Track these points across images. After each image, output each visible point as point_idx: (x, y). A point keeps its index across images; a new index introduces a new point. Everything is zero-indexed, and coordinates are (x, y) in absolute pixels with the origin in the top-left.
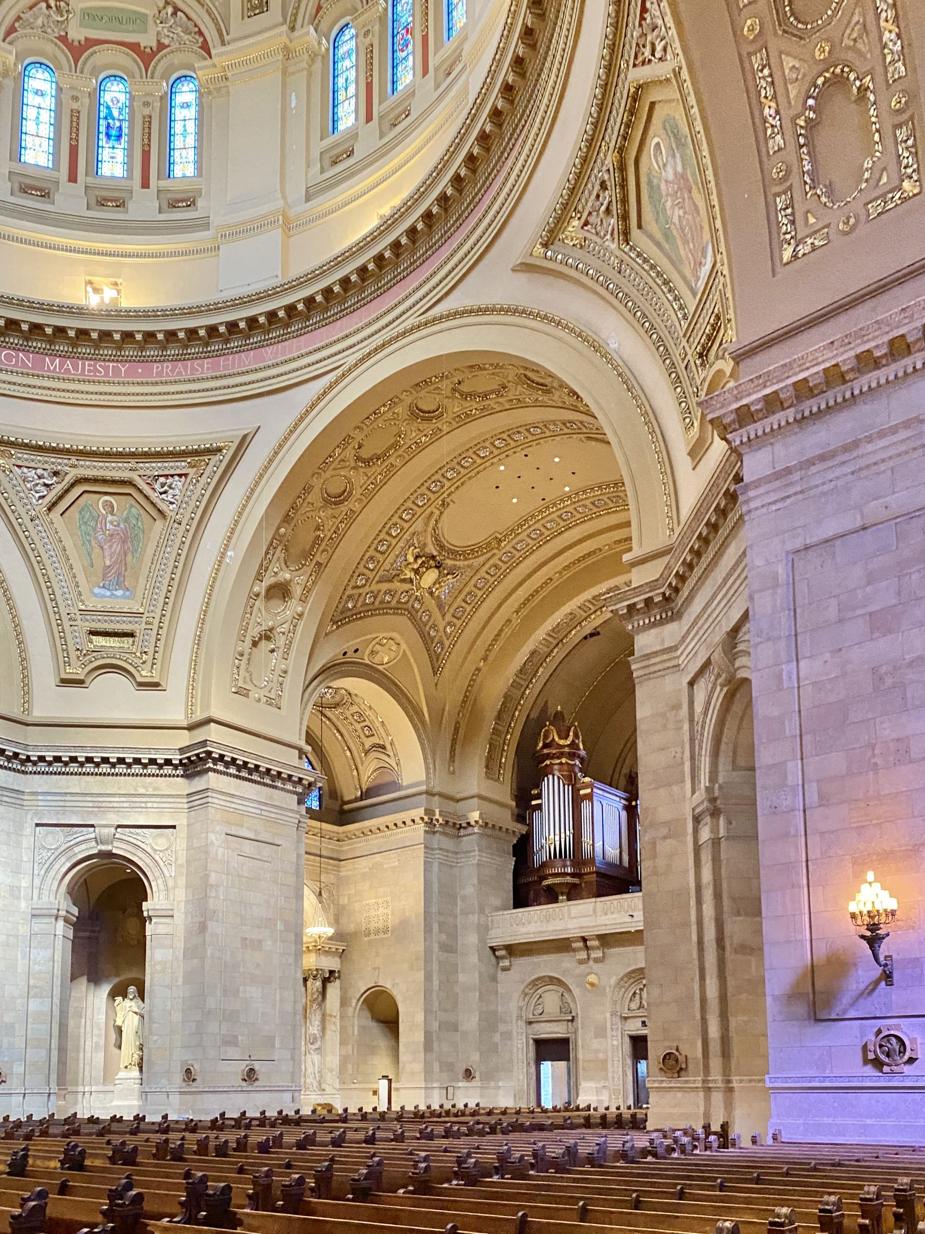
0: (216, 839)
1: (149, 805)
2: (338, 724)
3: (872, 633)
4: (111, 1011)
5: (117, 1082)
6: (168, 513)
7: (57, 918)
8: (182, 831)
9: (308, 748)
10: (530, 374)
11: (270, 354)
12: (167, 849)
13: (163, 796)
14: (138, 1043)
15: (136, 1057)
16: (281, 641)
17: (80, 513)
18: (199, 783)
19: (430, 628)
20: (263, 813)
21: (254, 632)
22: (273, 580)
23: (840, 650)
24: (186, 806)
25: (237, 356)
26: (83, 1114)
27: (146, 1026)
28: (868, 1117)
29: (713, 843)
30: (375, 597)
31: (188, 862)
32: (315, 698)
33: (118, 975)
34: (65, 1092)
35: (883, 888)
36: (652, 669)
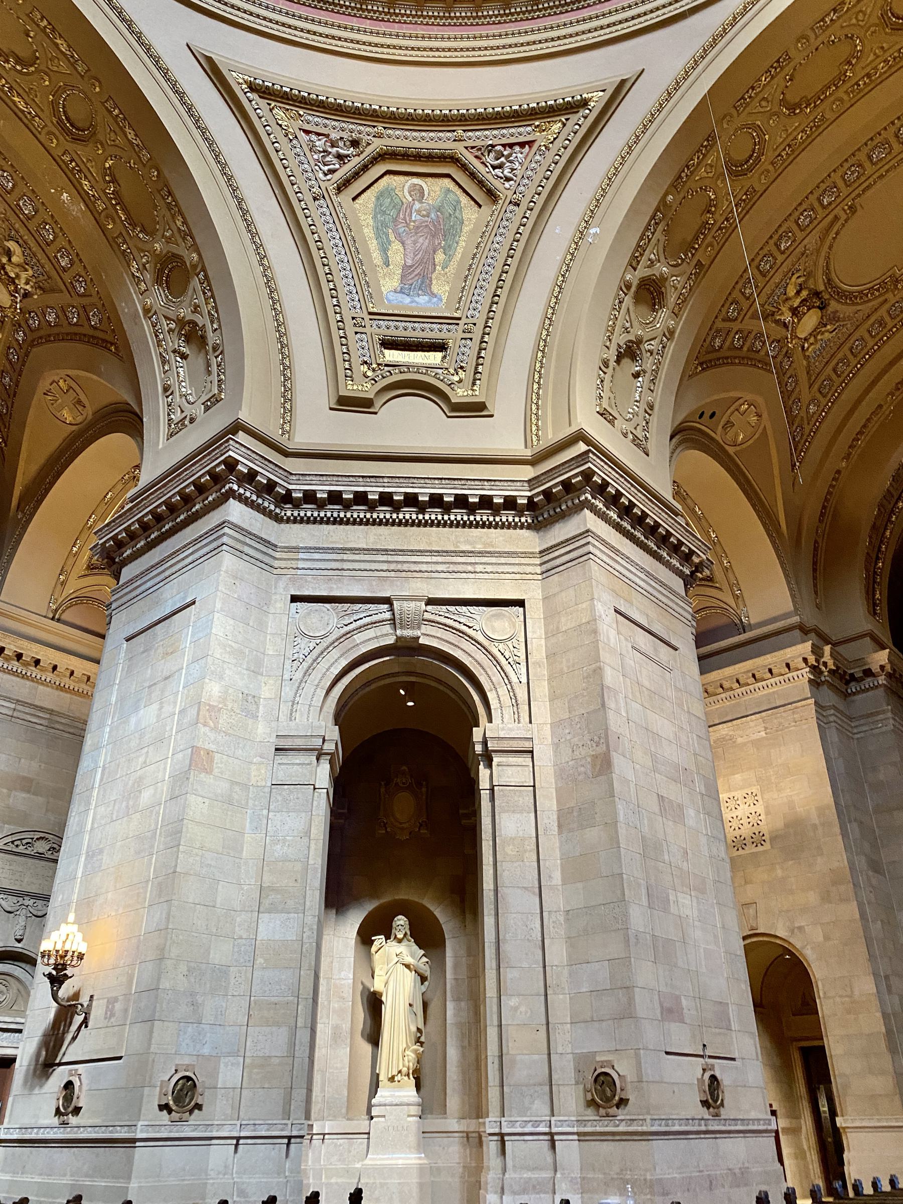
1: (479, 568)
12: (510, 639)
13: (500, 554)
17: (378, 199)
24: (538, 570)
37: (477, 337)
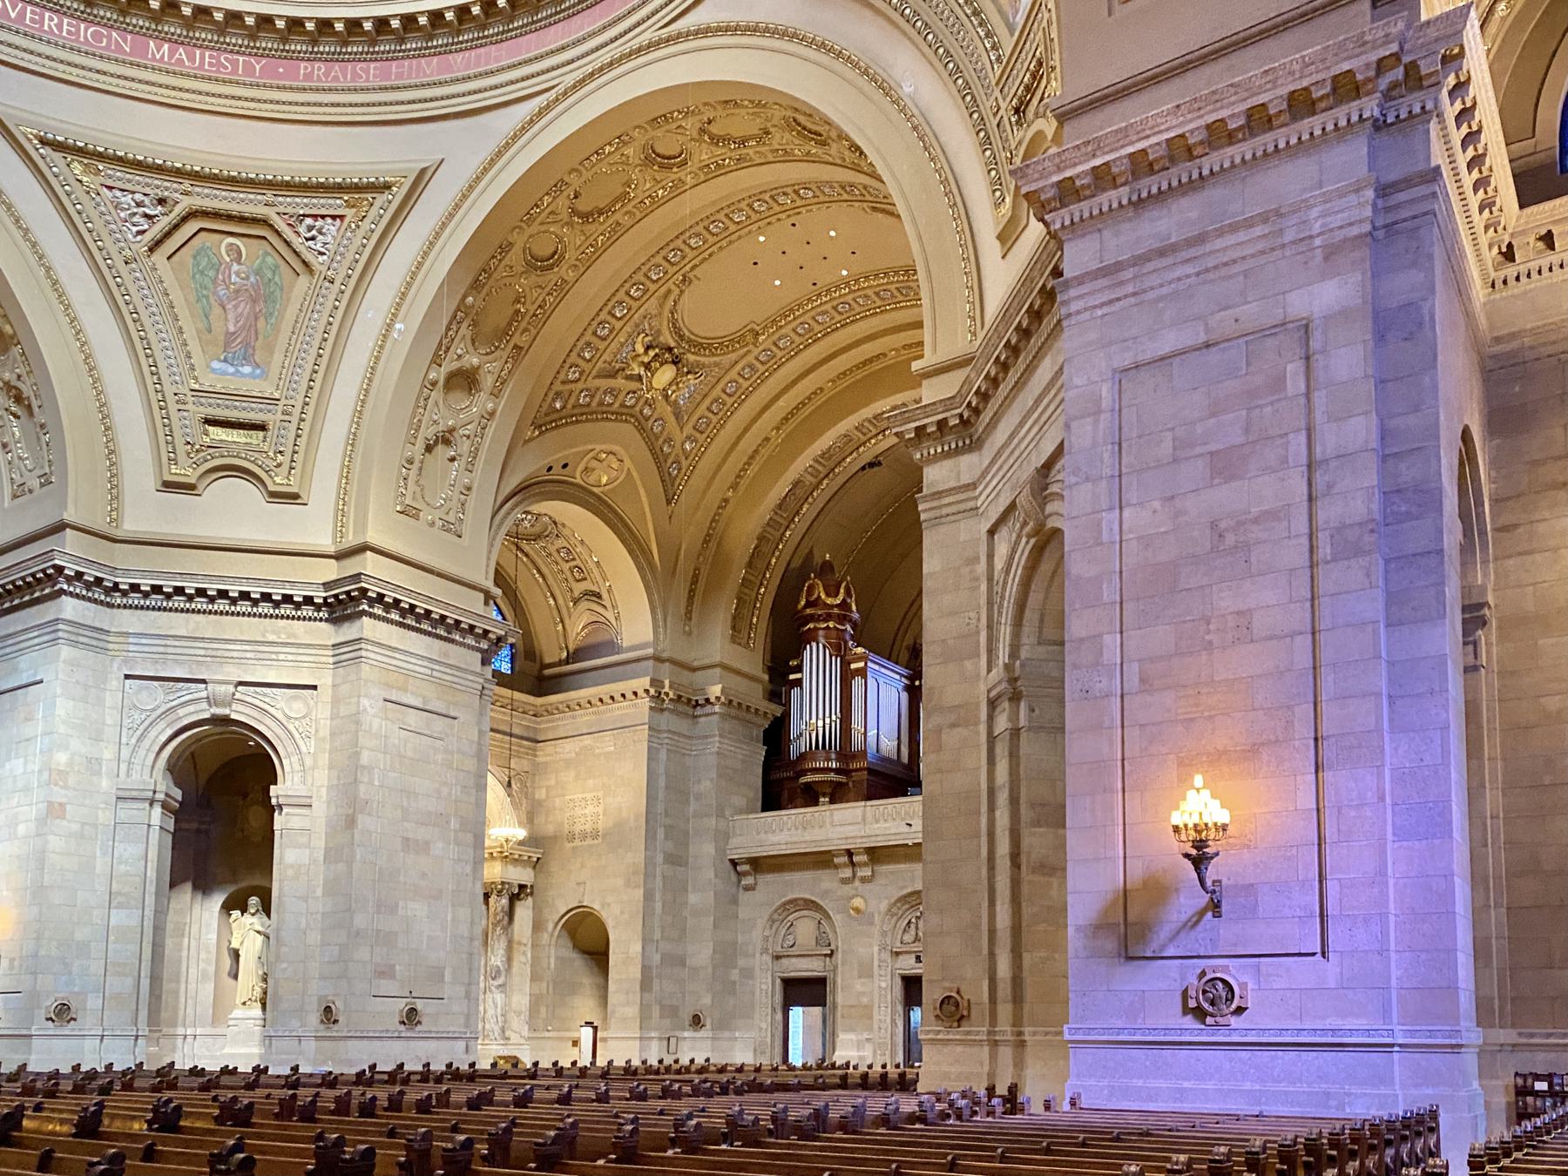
0: (370, 705)
1: (282, 657)
2: (539, 562)
3: (1212, 478)
4: (225, 930)
5: (231, 1023)
6: (316, 267)
7: (152, 802)
8: (325, 693)
9: (498, 592)
10: (801, 119)
11: (460, 62)
12: (304, 717)
14: (261, 973)
15: (258, 991)
16: (465, 447)
18: (349, 631)
19: (665, 441)
20: (435, 673)
21: (428, 432)
22: (455, 365)
23: (1172, 498)
24: (331, 660)
25: (414, 62)
26: (183, 1064)
27: (273, 948)
28: (1185, 1079)
29: (1011, 734)
30: (592, 397)
31: (332, 734)
32: (509, 523)
33: (235, 882)
34: (157, 1035)
35: (1213, 796)
36: (945, 511)
37: (295, 420)
